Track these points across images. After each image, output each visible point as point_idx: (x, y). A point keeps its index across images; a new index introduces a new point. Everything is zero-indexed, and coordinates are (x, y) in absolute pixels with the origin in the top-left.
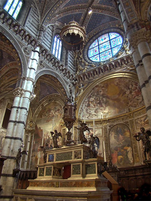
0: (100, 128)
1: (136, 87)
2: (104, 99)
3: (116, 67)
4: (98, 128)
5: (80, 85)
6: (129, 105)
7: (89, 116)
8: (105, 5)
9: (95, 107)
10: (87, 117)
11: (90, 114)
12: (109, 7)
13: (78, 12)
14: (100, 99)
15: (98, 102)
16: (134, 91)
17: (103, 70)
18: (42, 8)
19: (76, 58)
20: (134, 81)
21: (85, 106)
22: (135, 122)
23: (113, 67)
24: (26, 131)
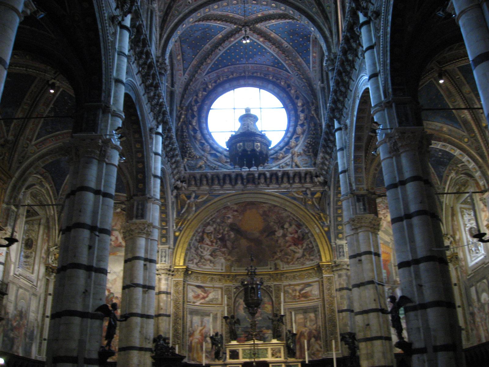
0: (217, 288)
1: (297, 229)
2: (232, 233)
3: (271, 182)
4: (214, 287)
5: (191, 194)
6: (276, 257)
7: (200, 261)
8: (276, 35)
9: (212, 245)
10: (197, 264)
11: (201, 257)
12: (284, 41)
13: (219, 24)
14: (224, 230)
15: (220, 236)
16: (291, 234)
17: (245, 181)
18: (164, 8)
19: (182, 121)
20: (297, 220)
21: (196, 240)
22: (284, 290)
23: (266, 181)
24: (47, 268)
